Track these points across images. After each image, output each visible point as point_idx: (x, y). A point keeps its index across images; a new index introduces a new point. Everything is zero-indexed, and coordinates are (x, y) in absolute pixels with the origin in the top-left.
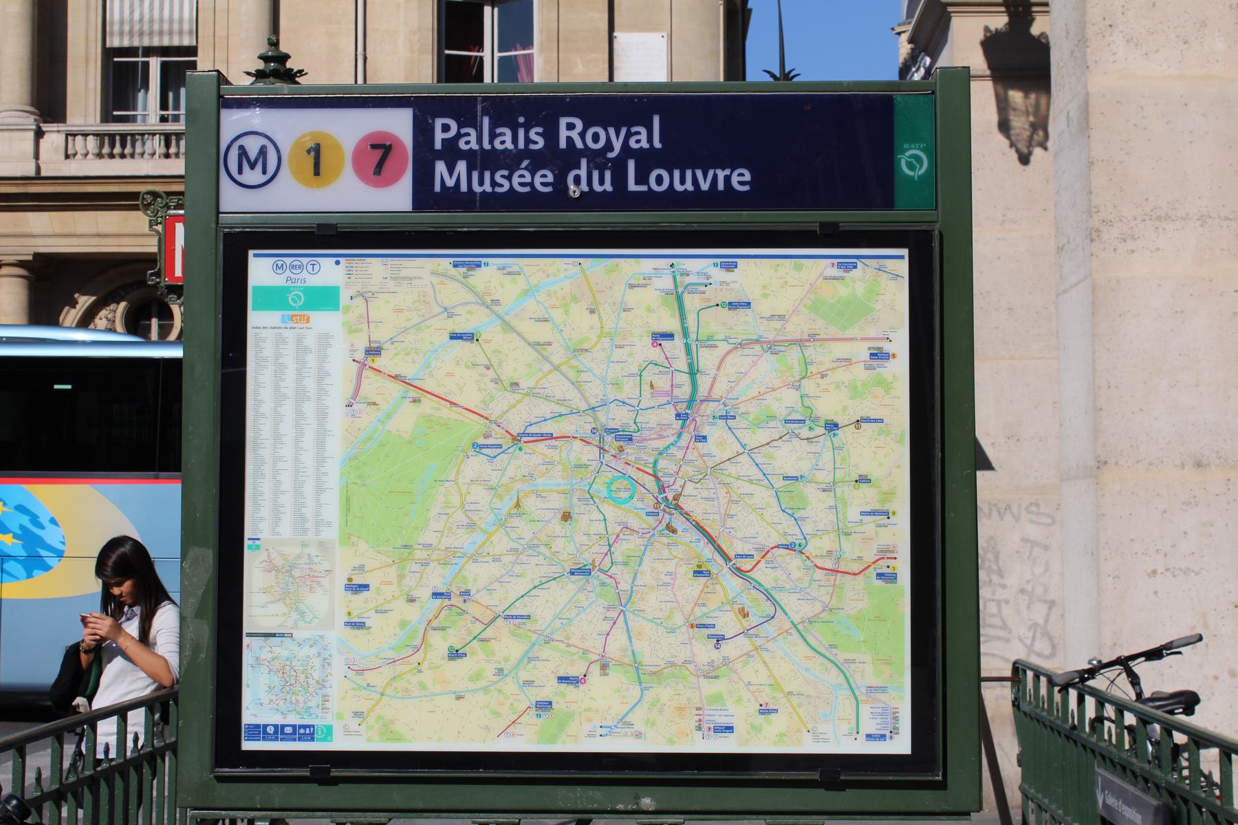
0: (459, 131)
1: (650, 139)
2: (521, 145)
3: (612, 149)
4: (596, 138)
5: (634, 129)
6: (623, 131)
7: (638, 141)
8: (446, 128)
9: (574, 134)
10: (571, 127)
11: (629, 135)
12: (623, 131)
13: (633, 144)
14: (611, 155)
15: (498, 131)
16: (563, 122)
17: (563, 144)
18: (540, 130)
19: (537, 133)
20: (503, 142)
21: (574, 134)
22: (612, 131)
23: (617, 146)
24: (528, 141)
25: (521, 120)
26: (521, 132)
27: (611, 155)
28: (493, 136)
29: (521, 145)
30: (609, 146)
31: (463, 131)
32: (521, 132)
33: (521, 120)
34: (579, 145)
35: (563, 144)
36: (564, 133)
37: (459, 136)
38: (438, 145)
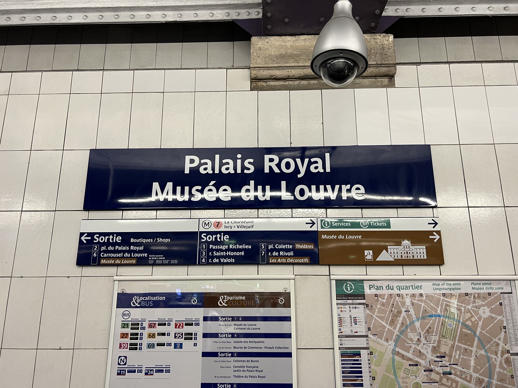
0: (200, 162)
1: (324, 167)
2: (239, 171)
3: (299, 173)
4: (288, 165)
5: (313, 160)
6: (306, 160)
7: (316, 168)
8: (192, 161)
9: (273, 165)
10: (271, 160)
11: (310, 163)
12: (306, 160)
13: (312, 169)
14: (299, 176)
15: (224, 161)
16: (267, 157)
17: (267, 170)
18: (252, 160)
19: (249, 163)
20: (227, 169)
21: (273, 165)
22: (298, 161)
23: (303, 171)
24: (243, 168)
25: (239, 156)
26: (239, 162)
27: (299, 176)
28: (221, 165)
29: (239, 171)
30: (297, 170)
31: (203, 161)
32: (239, 162)
33: (239, 156)
34: (277, 170)
35: (267, 170)
36: (267, 165)
37: (200, 164)
38: (187, 171)
